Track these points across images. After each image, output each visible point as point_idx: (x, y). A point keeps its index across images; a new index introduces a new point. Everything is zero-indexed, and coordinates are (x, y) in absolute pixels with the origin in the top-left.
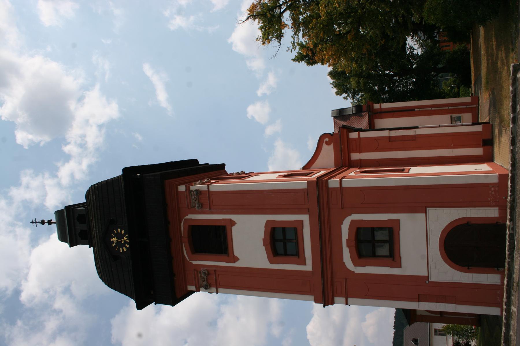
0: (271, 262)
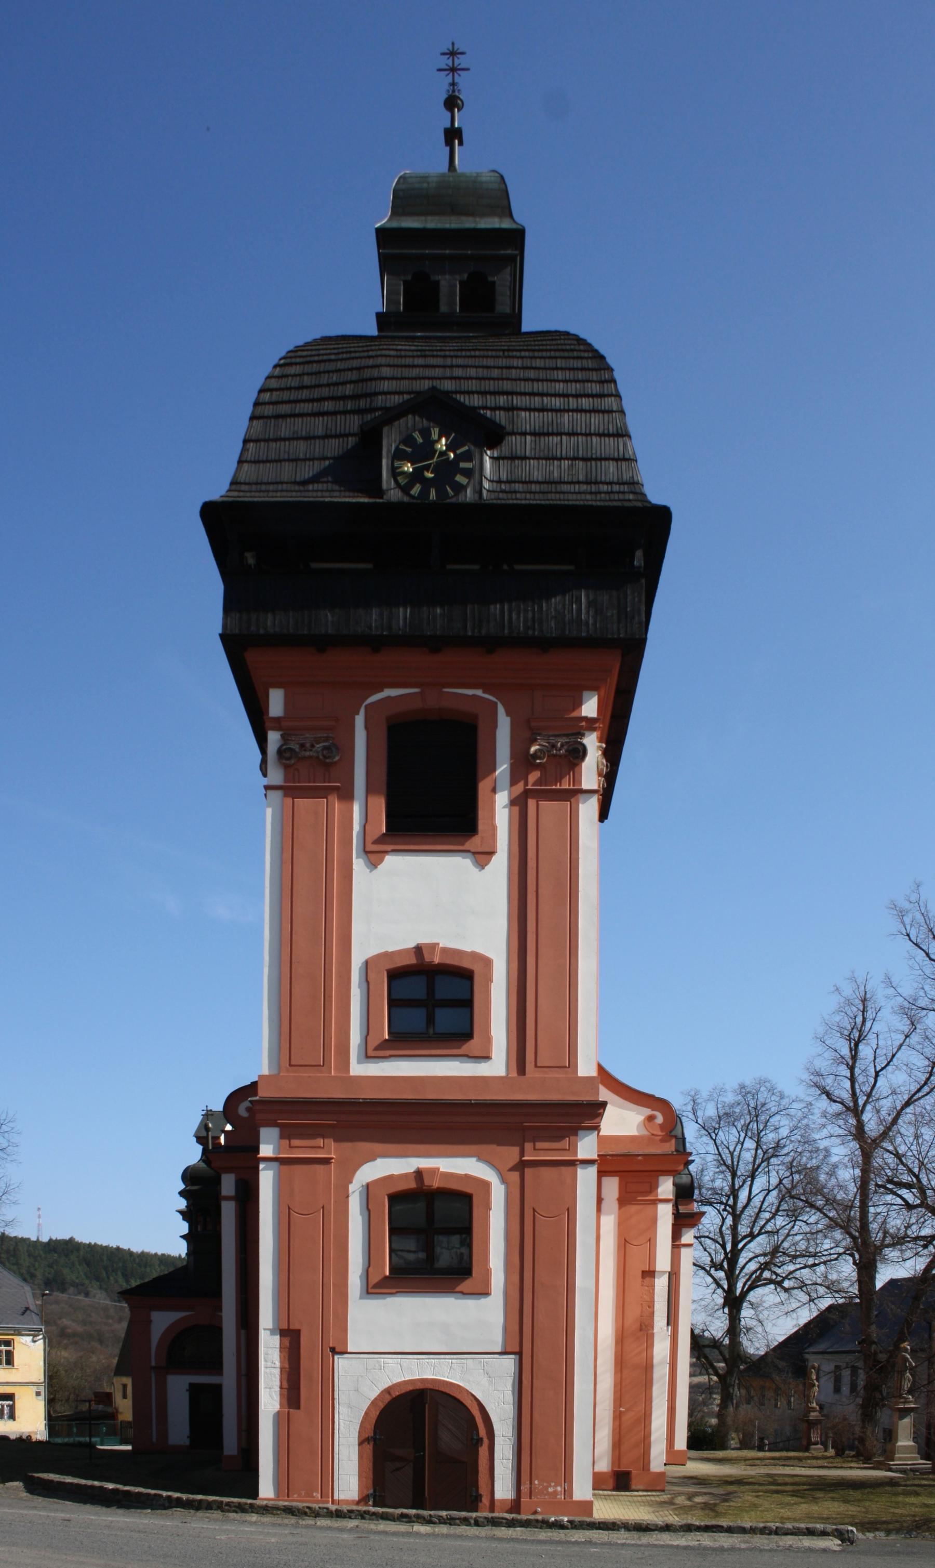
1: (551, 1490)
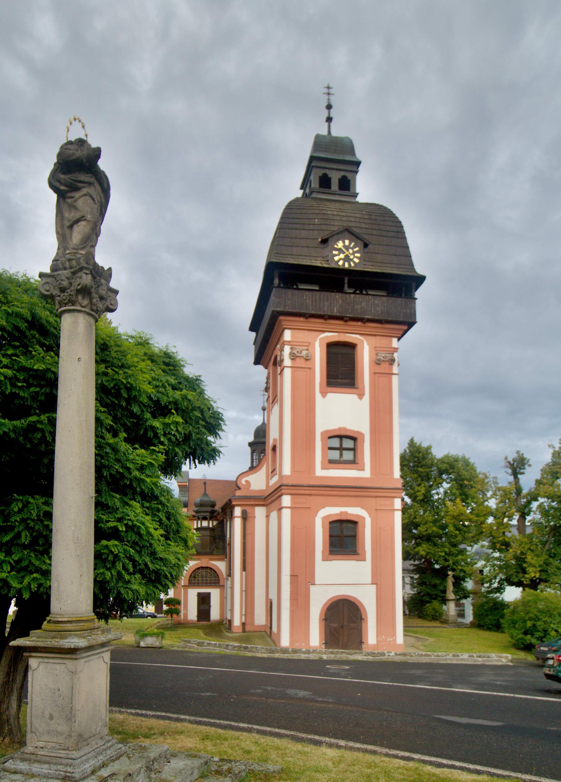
0: (323, 434)
1: (389, 640)
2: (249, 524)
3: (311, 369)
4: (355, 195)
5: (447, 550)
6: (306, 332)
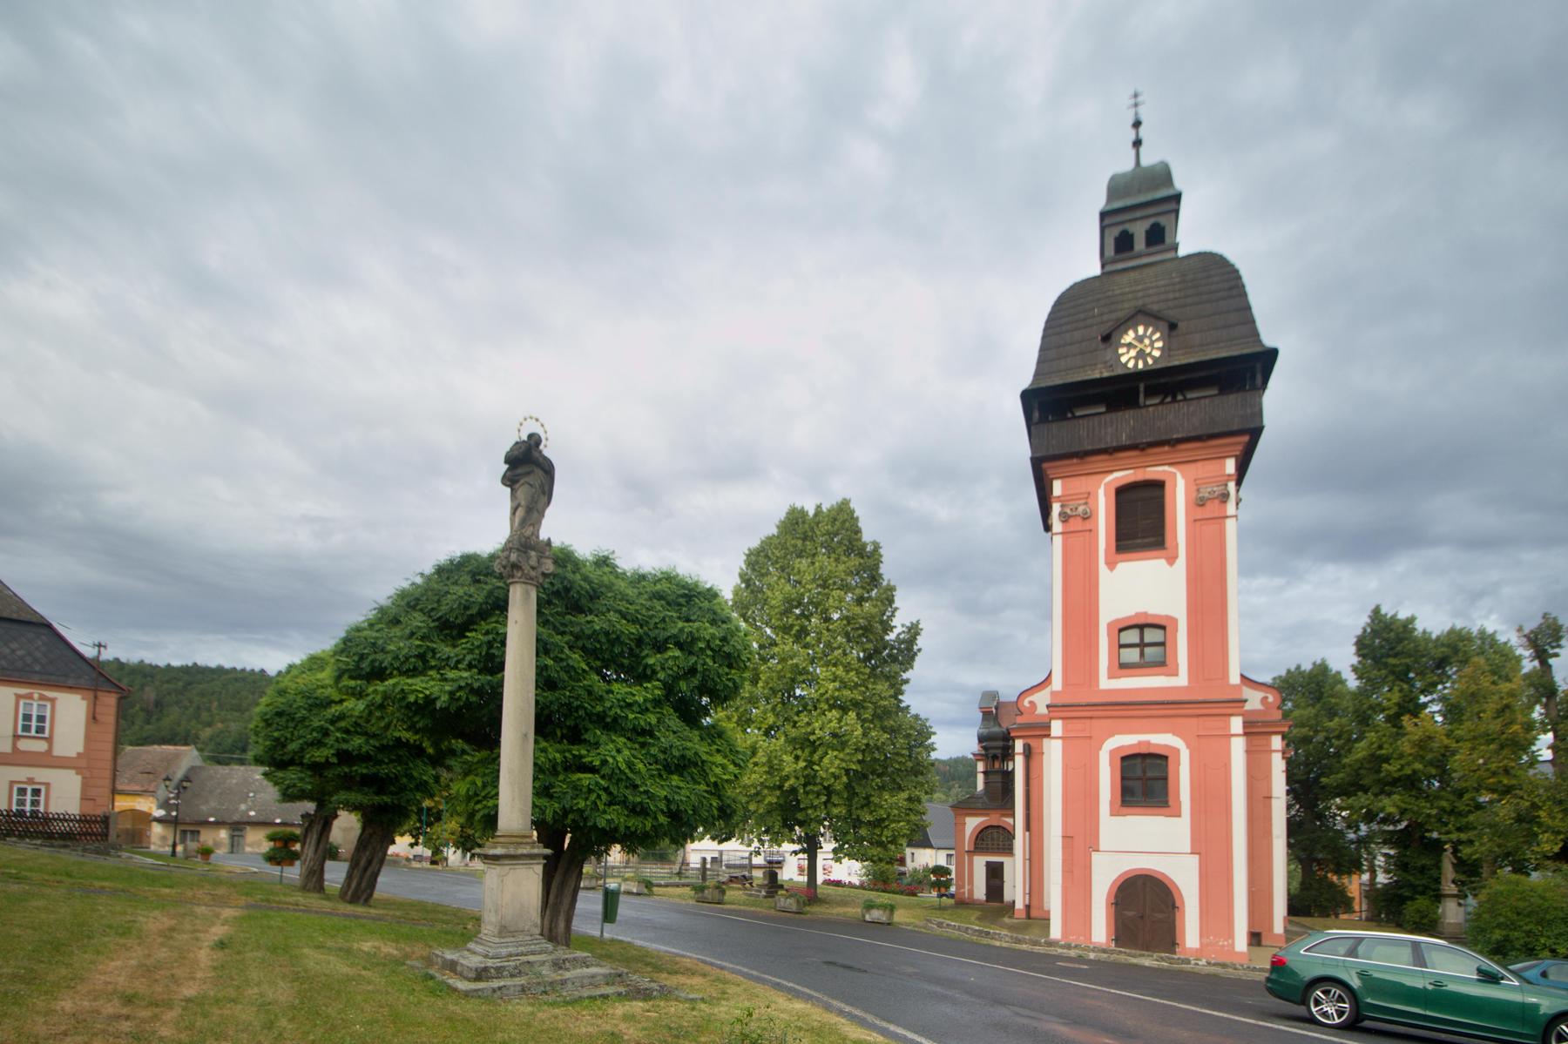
0: (1110, 625)
2: (1033, 764)
3: (1092, 532)
4: (1175, 248)
5: (1444, 804)
6: (1083, 478)
